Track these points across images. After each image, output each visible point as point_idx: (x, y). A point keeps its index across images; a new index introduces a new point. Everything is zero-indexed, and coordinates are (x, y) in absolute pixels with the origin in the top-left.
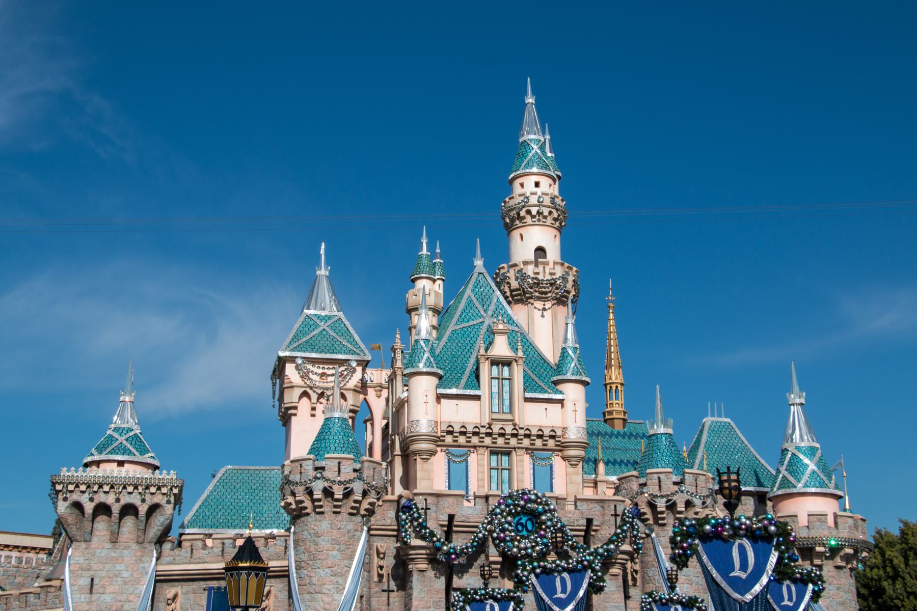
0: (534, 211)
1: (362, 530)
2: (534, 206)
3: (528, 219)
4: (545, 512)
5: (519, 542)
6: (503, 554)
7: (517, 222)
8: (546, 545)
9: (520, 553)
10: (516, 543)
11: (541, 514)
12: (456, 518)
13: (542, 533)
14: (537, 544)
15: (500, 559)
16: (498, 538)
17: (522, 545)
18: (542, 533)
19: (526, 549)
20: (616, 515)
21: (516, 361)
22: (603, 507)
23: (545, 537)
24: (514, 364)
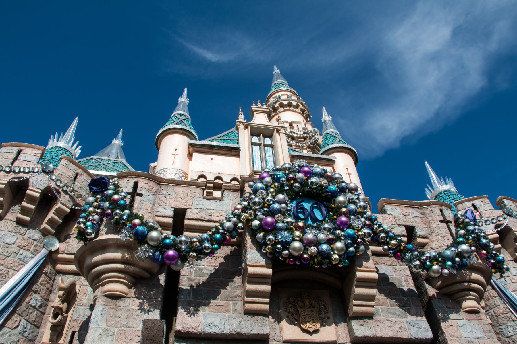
0: (285, 103)
1: (38, 252)
2: (285, 100)
3: (282, 109)
4: (342, 190)
5: (303, 230)
6: (274, 259)
7: (273, 114)
8: (354, 239)
9: (306, 250)
10: (298, 233)
11: (335, 194)
12: (188, 214)
13: (344, 219)
14: (338, 238)
15: (270, 271)
16: (261, 228)
17: (310, 236)
18: (344, 219)
19: (317, 243)
20: (447, 222)
21: (278, 131)
22: (424, 214)
23: (350, 227)
24: (276, 134)
